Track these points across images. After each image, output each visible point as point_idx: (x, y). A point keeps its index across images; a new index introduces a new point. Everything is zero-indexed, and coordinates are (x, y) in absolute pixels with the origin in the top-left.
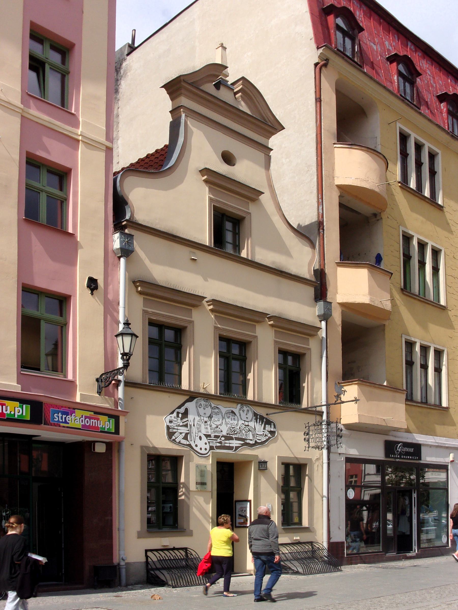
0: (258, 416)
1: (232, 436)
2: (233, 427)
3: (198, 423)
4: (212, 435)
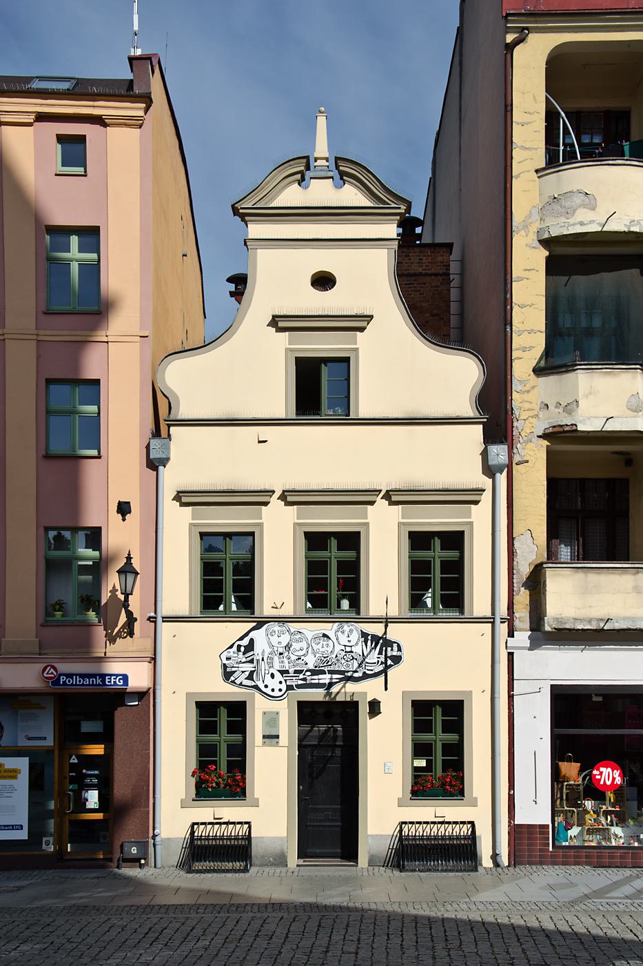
0: (369, 637)
1: (323, 668)
2: (324, 656)
3: (270, 656)
4: (291, 670)
